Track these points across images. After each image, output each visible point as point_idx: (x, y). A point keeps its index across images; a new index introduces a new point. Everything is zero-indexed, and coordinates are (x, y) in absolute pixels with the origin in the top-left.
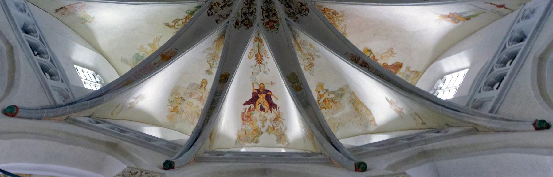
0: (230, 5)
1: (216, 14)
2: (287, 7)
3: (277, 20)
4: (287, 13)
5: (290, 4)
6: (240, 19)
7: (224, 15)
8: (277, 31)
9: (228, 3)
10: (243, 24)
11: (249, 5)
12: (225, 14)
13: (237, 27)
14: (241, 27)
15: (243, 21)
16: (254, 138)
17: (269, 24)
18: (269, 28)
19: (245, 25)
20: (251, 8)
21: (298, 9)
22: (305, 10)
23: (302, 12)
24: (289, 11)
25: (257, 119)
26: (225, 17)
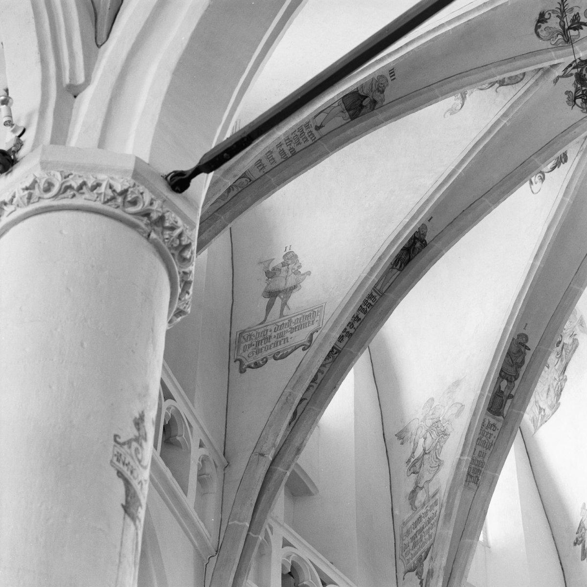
7: (572, 9)
12: (576, 11)
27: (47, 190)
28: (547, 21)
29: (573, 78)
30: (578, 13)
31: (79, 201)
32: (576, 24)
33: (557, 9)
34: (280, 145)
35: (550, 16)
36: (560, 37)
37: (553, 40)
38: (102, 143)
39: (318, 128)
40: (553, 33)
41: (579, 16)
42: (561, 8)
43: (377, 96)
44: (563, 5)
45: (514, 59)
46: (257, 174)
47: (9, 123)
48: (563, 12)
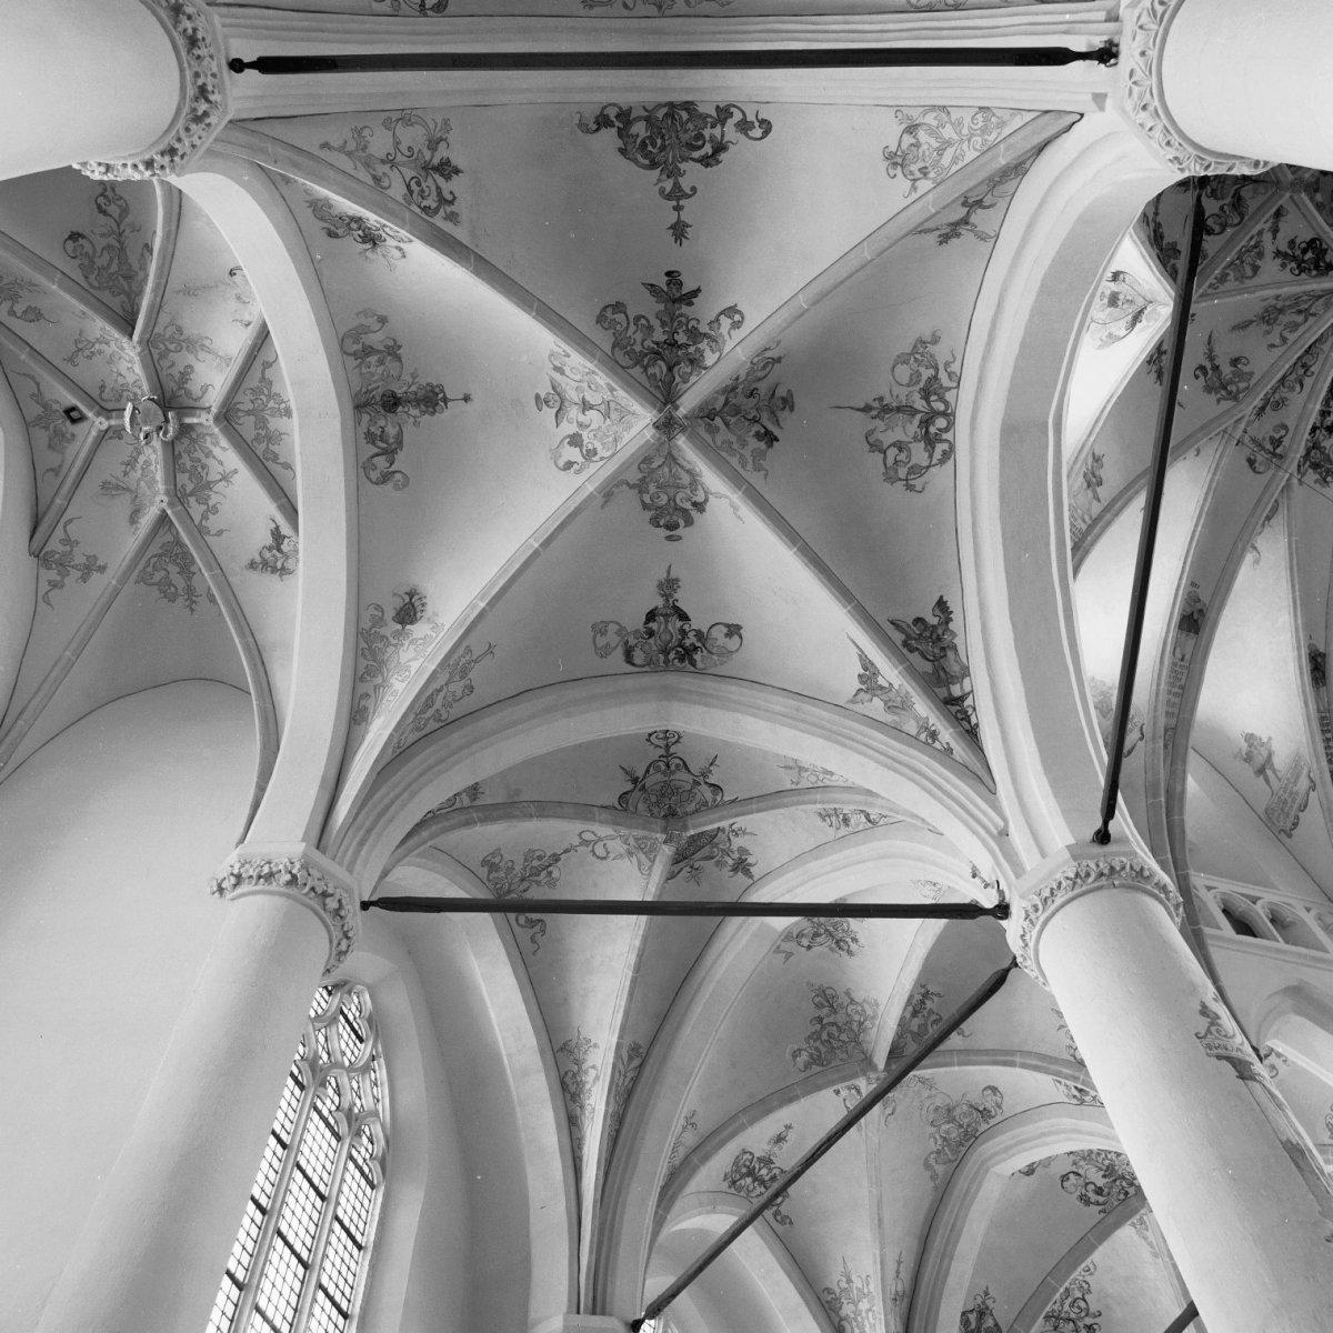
0: (1278, 405)
7: (1264, 439)
15: (1308, 453)
19: (1315, 466)
20: (1329, 413)
26: (1269, 447)
27: (1037, 910)
29: (1310, 471)
31: (1059, 901)
34: (1170, 692)
36: (1274, 460)
38: (1043, 854)
39: (1182, 660)
43: (1199, 606)
45: (1259, 501)
46: (1173, 722)
47: (986, 886)
48: (1260, 446)
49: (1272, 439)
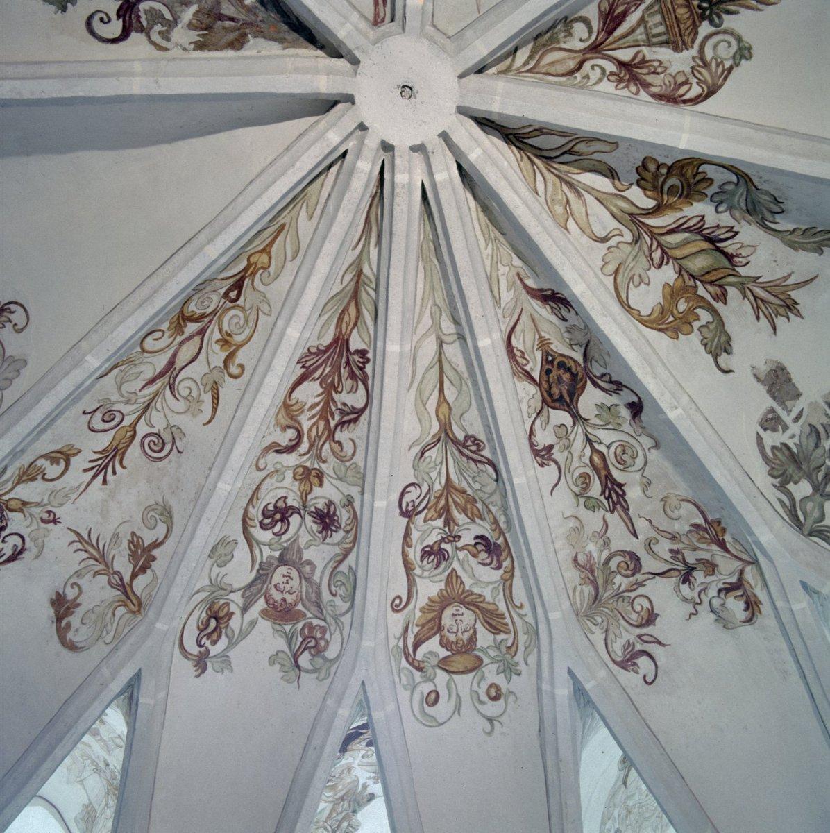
0: (160, 446)
1: (58, 538)
2: (592, 505)
3: (502, 607)
4: (587, 570)
5: (616, 474)
6: (240, 571)
7: (116, 536)
8: (492, 709)
9: (142, 429)
10: (261, 604)
11: (305, 446)
13: (215, 650)
14: (244, 635)
15: (263, 574)
16: (339, 826)
17: (447, 620)
18: (444, 664)
19: (281, 613)
21: (673, 538)
22: (728, 589)
23: (699, 576)
24: (603, 537)
25: (355, 765)
28: (79, 601)
29: (265, 626)
30: (133, 534)
32: (142, 556)
33: (83, 565)
35: (79, 587)
36: (121, 611)
37: (108, 633)
40: (103, 616)
41: (138, 537)
42: (91, 554)
44: (93, 546)
49: (135, 541)
